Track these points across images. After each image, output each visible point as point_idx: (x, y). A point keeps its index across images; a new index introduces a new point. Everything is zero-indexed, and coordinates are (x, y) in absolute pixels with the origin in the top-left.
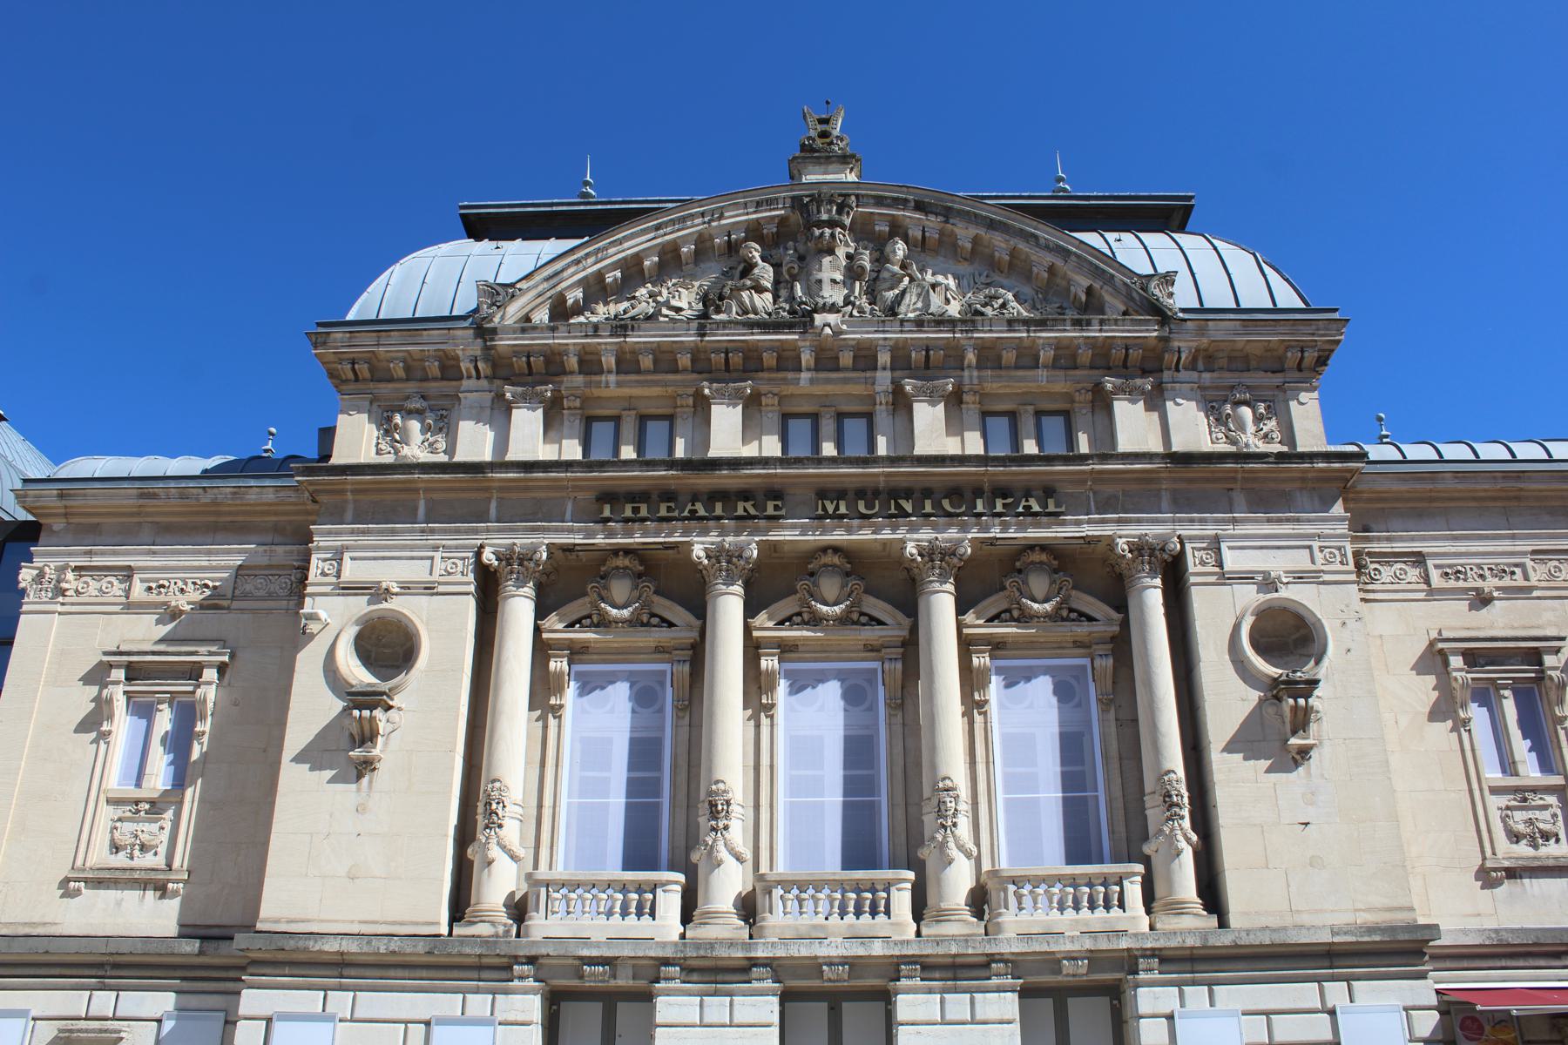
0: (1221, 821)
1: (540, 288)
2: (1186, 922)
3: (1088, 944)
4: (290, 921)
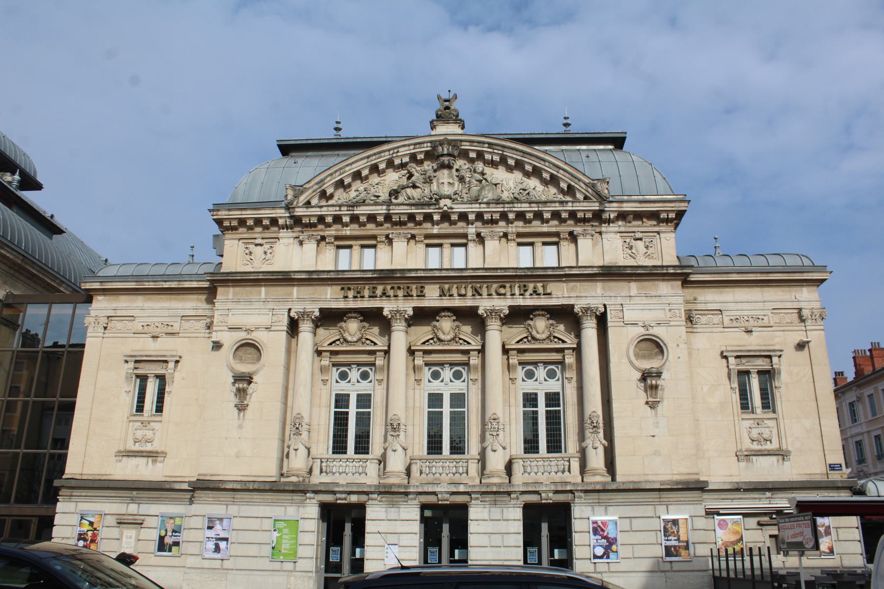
0: (616, 434)
1: (315, 187)
2: (598, 479)
3: (553, 488)
4: (212, 475)
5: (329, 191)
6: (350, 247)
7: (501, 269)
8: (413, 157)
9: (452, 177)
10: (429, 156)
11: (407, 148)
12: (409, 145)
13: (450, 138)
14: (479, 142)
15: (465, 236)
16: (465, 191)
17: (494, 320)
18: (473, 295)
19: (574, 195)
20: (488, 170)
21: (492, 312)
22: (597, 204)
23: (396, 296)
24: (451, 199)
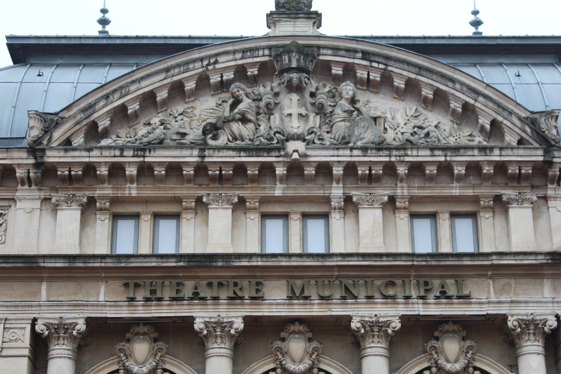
1: (78, 117)
5: (103, 124)
6: (136, 216)
7: (388, 255)
8: (241, 72)
9: (304, 105)
10: (266, 71)
11: (231, 57)
12: (235, 52)
13: (300, 42)
14: (348, 50)
15: (327, 200)
16: (325, 128)
17: (376, 340)
18: (343, 298)
19: (502, 136)
20: (363, 97)
21: (376, 327)
22: (541, 152)
23: (216, 298)
24: (304, 140)
